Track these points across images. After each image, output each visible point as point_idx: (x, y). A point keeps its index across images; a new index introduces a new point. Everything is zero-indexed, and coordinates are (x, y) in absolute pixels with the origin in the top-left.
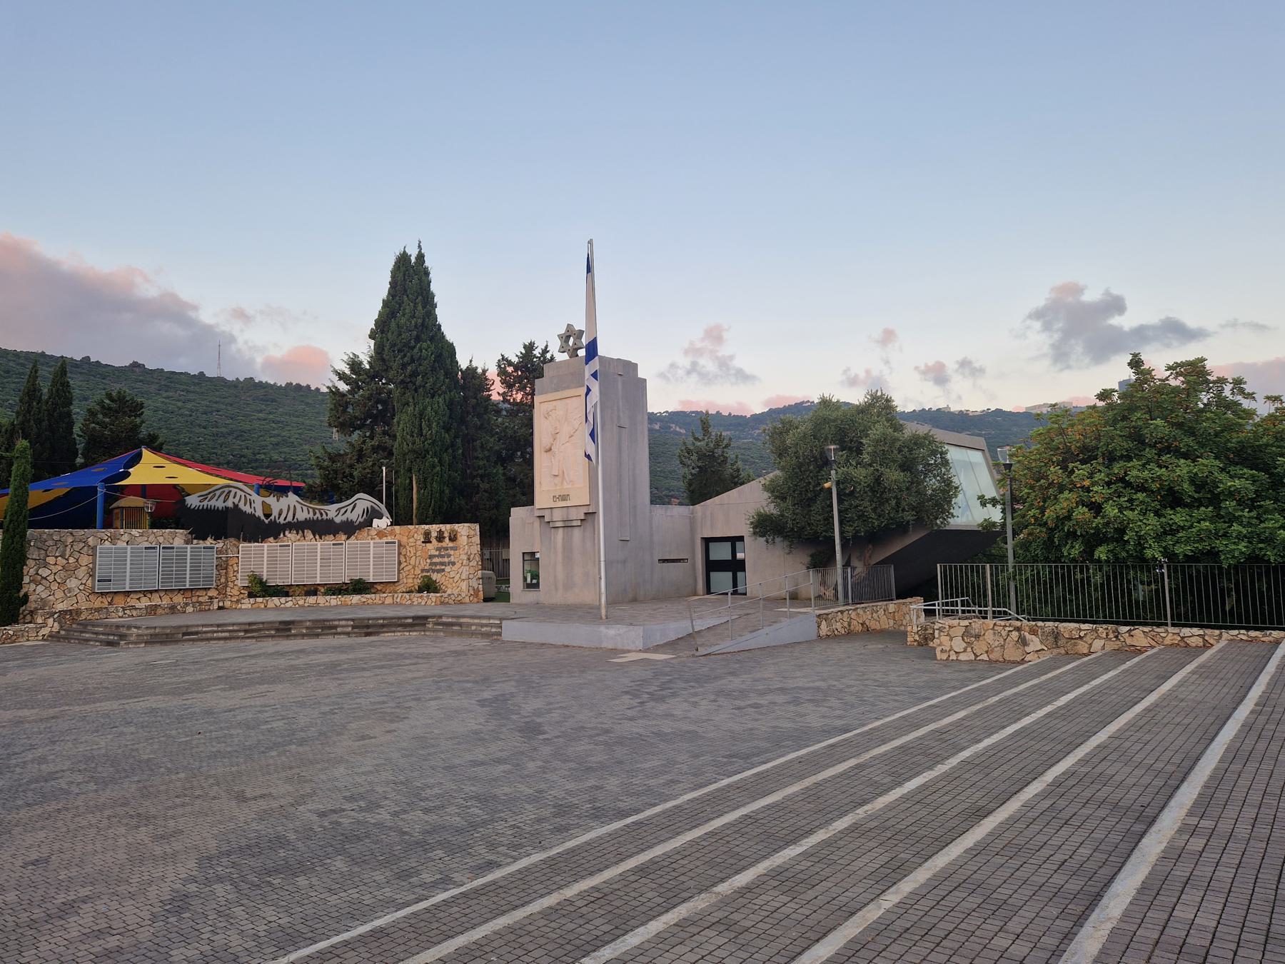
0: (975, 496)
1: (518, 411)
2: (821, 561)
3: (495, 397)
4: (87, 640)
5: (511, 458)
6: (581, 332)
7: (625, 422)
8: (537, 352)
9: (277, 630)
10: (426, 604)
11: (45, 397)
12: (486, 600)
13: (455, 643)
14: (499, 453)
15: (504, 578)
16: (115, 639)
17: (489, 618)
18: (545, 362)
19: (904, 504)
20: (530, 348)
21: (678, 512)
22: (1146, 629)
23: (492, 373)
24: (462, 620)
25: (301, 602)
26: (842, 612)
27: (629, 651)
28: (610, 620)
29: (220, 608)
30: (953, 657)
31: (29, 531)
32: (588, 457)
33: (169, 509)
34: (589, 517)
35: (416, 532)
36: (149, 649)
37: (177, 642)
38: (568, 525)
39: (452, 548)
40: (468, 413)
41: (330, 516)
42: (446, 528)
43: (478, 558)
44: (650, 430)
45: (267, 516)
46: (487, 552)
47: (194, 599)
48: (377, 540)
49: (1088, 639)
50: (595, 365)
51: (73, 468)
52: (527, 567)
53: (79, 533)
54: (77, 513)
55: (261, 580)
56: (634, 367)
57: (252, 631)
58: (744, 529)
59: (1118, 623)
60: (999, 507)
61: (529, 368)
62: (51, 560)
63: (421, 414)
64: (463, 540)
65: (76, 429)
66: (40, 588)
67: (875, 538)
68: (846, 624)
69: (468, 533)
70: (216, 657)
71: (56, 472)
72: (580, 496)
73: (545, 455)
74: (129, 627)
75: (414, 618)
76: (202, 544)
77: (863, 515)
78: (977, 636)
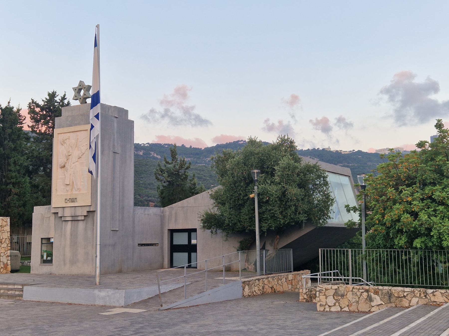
0: (343, 205)
1: (42, 139)
2: (247, 245)
3: (26, 128)
5: (36, 171)
6: (89, 87)
8: (58, 99)
12: (13, 271)
14: (27, 168)
15: (27, 255)
17: (14, 284)
18: (63, 106)
19: (300, 209)
20: (52, 95)
21: (153, 211)
22: (443, 291)
23: (25, 111)
26: (259, 280)
27: (114, 307)
30: (327, 309)
32: (91, 172)
34: (91, 214)
38: (75, 219)
40: (5, 139)
44: (136, 156)
46: (15, 238)
49: (409, 297)
50: (98, 109)
52: (44, 248)
58: (196, 224)
59: (426, 288)
60: (358, 213)
61: (51, 110)
67: (281, 231)
68: (261, 288)
72: (84, 200)
73: (60, 171)
77: (274, 216)
78: (342, 296)
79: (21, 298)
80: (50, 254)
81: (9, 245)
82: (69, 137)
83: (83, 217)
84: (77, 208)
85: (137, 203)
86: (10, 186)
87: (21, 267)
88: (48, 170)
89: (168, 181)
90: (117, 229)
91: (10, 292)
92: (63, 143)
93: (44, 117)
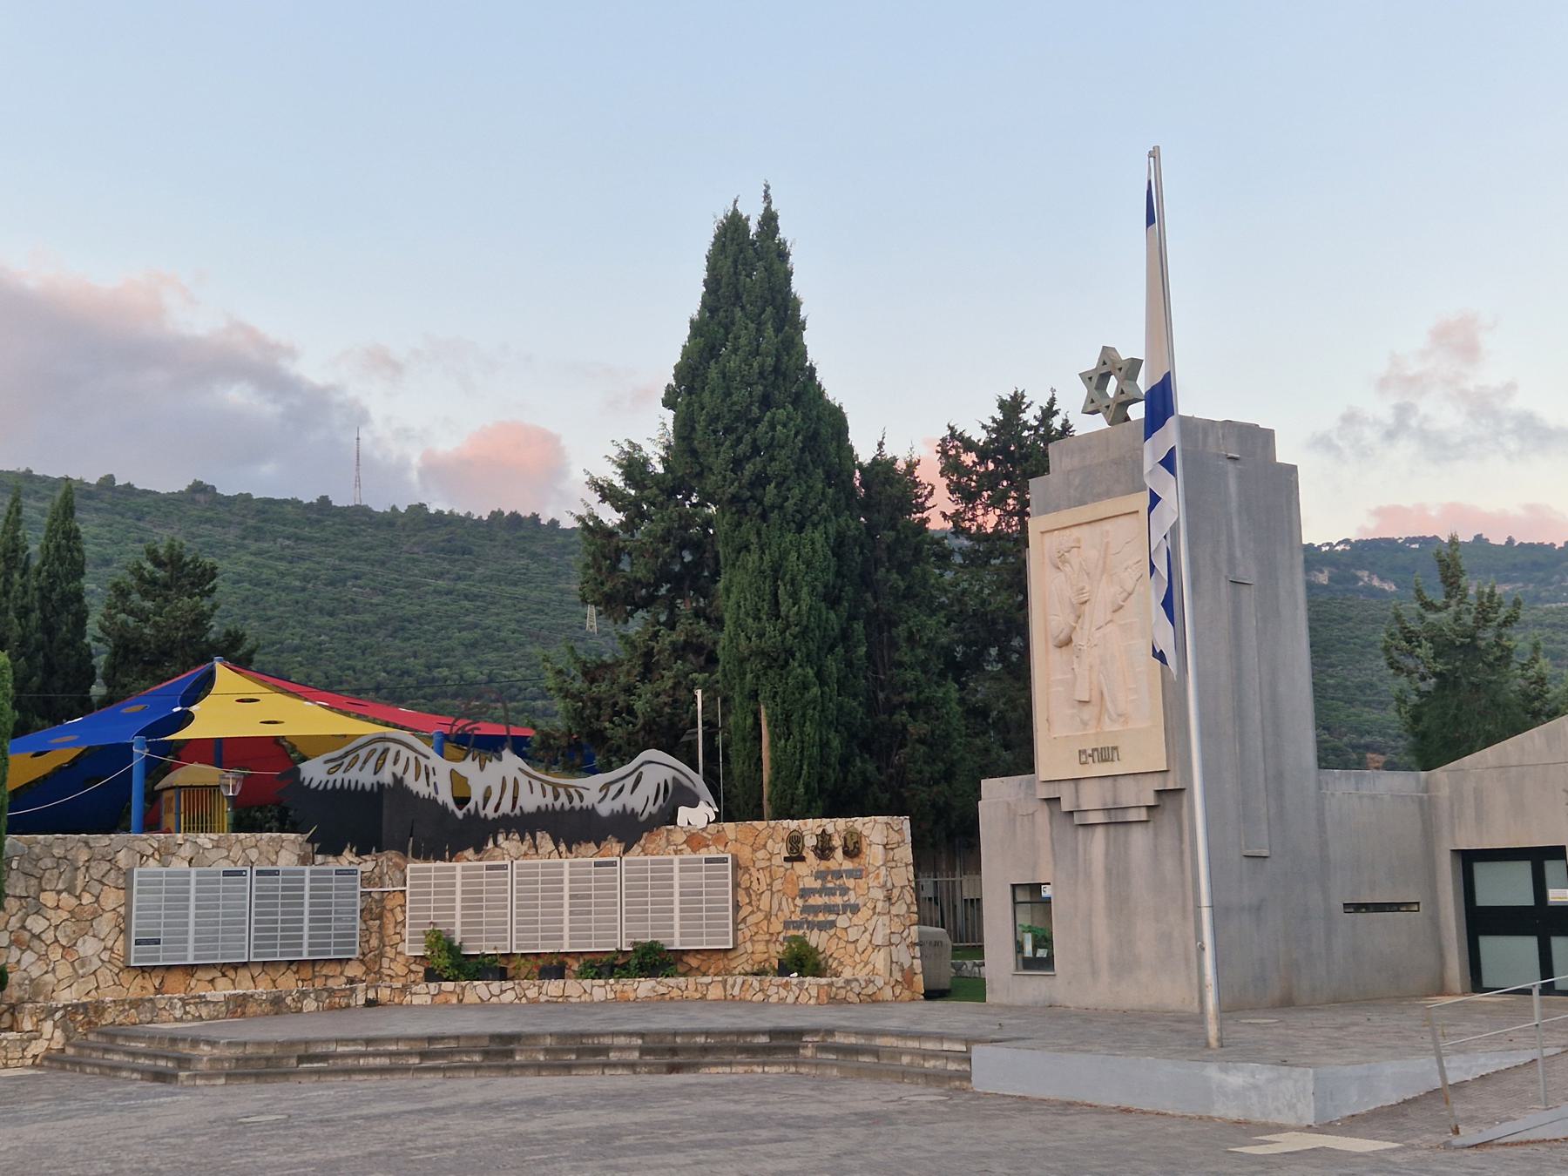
1: (990, 554)
3: (937, 524)
4: (116, 1068)
5: (975, 662)
6: (1135, 364)
7: (1248, 570)
8: (1030, 416)
9: (486, 1053)
10: (795, 1002)
11: (36, 562)
12: (930, 995)
13: (865, 1095)
14: (947, 652)
15: (969, 943)
16: (168, 1066)
17: (941, 1037)
18: (1049, 438)
21: (1388, 788)
23: (930, 472)
24: (879, 1041)
25: (532, 993)
28: (1230, 1051)
29: (370, 1003)
31: (10, 839)
32: (1160, 656)
33: (269, 789)
35: (773, 833)
36: (234, 1088)
37: (286, 1075)
38: (1116, 821)
39: (851, 874)
41: (587, 803)
42: (836, 826)
43: (909, 897)
44: (1311, 587)
45: (462, 801)
46: (927, 882)
47: (319, 984)
48: (688, 854)
50: (1170, 435)
51: (85, 706)
52: (1024, 919)
53: (101, 841)
54: (94, 800)
55: (450, 942)
56: (1268, 435)
57: (434, 1054)
62: (49, 898)
63: (777, 570)
64: (874, 854)
65: (92, 626)
66: (29, 957)
69: (884, 838)
70: (365, 1111)
71: (56, 716)
72: (1144, 751)
74: (195, 1042)
75: (774, 1033)
76: (333, 864)
79: (965, 1084)
80: (1043, 940)
81: (915, 909)
82: (1078, 540)
83: (1144, 811)
84: (1121, 781)
85: (1332, 756)
86: (902, 716)
87: (953, 982)
88: (1014, 657)
89: (1436, 674)
90: (1265, 853)
91: (930, 1064)
92: (1060, 562)
93: (990, 480)
